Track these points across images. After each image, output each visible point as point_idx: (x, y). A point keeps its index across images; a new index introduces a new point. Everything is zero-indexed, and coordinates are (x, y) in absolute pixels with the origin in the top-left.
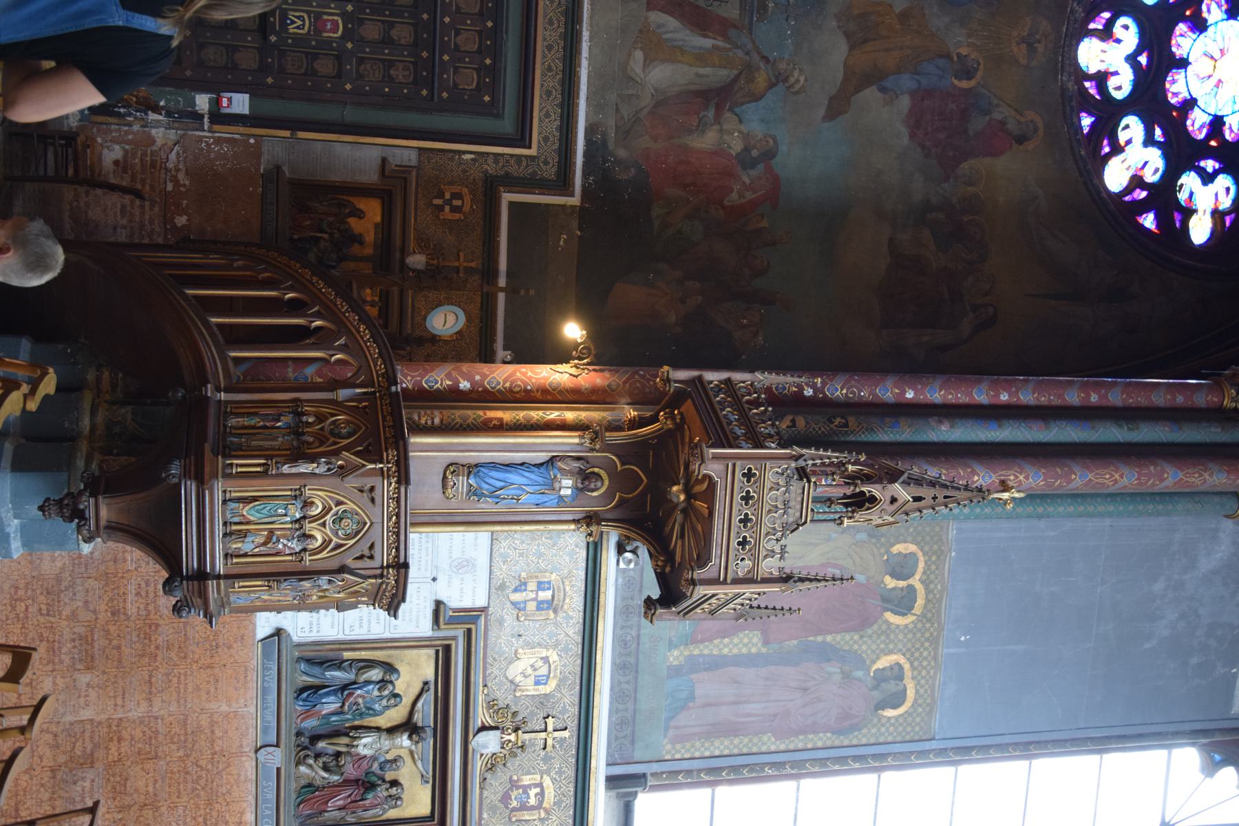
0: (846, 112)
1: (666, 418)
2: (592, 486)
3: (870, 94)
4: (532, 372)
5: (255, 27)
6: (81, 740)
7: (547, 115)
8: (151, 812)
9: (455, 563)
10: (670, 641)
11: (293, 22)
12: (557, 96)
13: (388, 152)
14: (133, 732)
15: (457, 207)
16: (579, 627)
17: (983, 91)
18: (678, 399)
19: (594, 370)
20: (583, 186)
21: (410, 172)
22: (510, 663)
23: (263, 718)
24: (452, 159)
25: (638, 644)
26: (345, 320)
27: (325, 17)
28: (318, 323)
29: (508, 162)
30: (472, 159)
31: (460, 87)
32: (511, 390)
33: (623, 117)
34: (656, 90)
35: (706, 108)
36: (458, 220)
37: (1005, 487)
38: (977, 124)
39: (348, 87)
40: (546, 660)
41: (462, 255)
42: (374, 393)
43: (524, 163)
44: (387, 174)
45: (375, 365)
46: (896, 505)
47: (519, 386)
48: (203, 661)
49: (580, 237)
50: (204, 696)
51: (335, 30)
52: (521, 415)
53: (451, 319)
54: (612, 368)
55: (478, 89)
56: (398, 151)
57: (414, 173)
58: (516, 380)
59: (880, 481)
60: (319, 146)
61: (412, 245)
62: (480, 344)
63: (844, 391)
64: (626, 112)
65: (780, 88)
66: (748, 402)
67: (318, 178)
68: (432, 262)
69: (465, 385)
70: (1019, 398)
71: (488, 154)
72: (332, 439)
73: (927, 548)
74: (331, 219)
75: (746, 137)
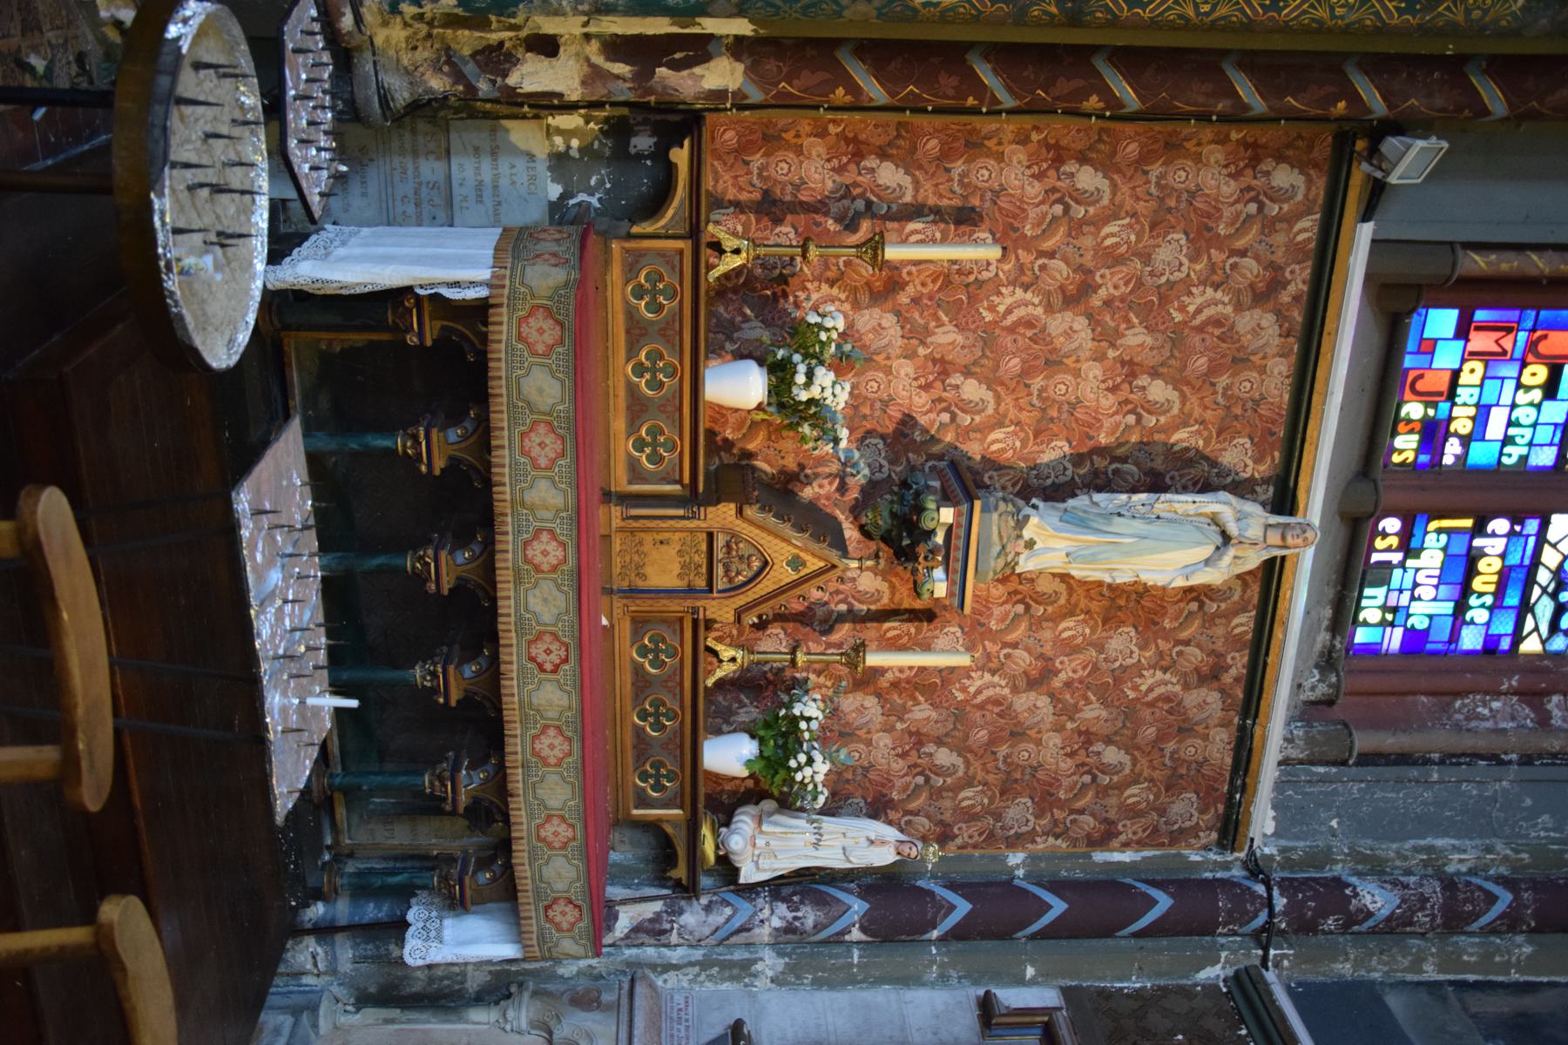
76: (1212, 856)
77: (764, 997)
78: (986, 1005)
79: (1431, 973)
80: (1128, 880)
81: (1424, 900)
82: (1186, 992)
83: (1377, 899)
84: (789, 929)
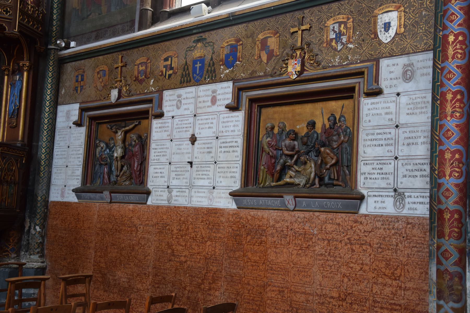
6: (98, 278)
8: (124, 251)
9: (67, 119)
10: (99, 14)
14: (98, 256)
16: (89, 60)
22: (97, 89)
23: (98, 200)
25: (99, 30)
40: (98, 73)
48: (81, 225)
50: (91, 225)
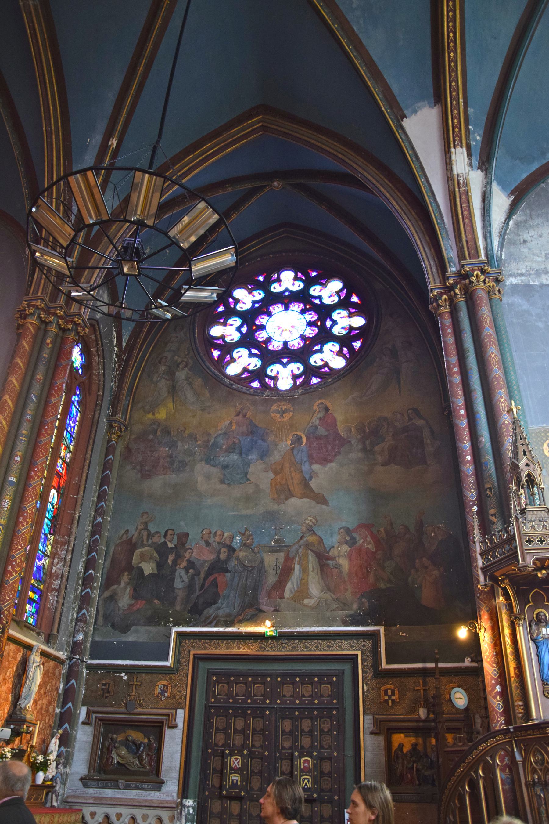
0: (323, 495)
1: (504, 583)
2: (543, 617)
3: (313, 484)
4: (486, 652)
5: (310, 805)
7: (340, 646)
11: (306, 784)
12: (330, 642)
13: (367, 731)
15: (391, 693)
17: (306, 431)
18: (494, 579)
19: (480, 620)
20: (374, 625)
21: (377, 719)
24: (367, 696)
26: (477, 758)
27: (302, 767)
28: (481, 772)
29: (365, 666)
30: (366, 685)
31: (330, 693)
32: (497, 663)
33: (337, 607)
34: (322, 591)
35: (328, 565)
36: (399, 692)
37: (510, 411)
38: (322, 431)
39: (335, 754)
41: (417, 688)
42: (515, 741)
43: (365, 657)
44: (379, 732)
45: (500, 740)
46: (530, 463)
47: (494, 659)
49: (400, 625)
51: (307, 761)
52: (510, 657)
53: (458, 695)
54: (478, 610)
55: (330, 684)
56: (366, 726)
57: (377, 716)
58: (492, 661)
59: (519, 473)
60: (368, 770)
61: (415, 716)
62: (463, 675)
63: (472, 490)
64: (335, 606)
65: (315, 529)
66: (491, 544)
67: (384, 770)
68: (422, 705)
69: (498, 689)
70: (462, 405)
71: (363, 677)
72: (546, 764)
73: (544, 439)
74: (405, 762)
75: (340, 544)
76: (65, 667)
77: (73, 771)
78: (83, 723)
79: (92, 629)
80: (66, 687)
81: (82, 627)
82: (87, 680)
83: (80, 637)
84: (63, 765)
